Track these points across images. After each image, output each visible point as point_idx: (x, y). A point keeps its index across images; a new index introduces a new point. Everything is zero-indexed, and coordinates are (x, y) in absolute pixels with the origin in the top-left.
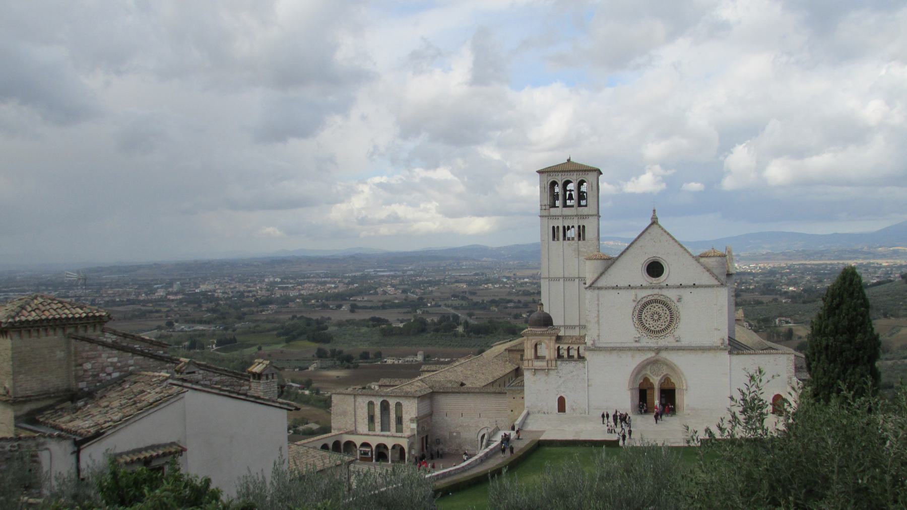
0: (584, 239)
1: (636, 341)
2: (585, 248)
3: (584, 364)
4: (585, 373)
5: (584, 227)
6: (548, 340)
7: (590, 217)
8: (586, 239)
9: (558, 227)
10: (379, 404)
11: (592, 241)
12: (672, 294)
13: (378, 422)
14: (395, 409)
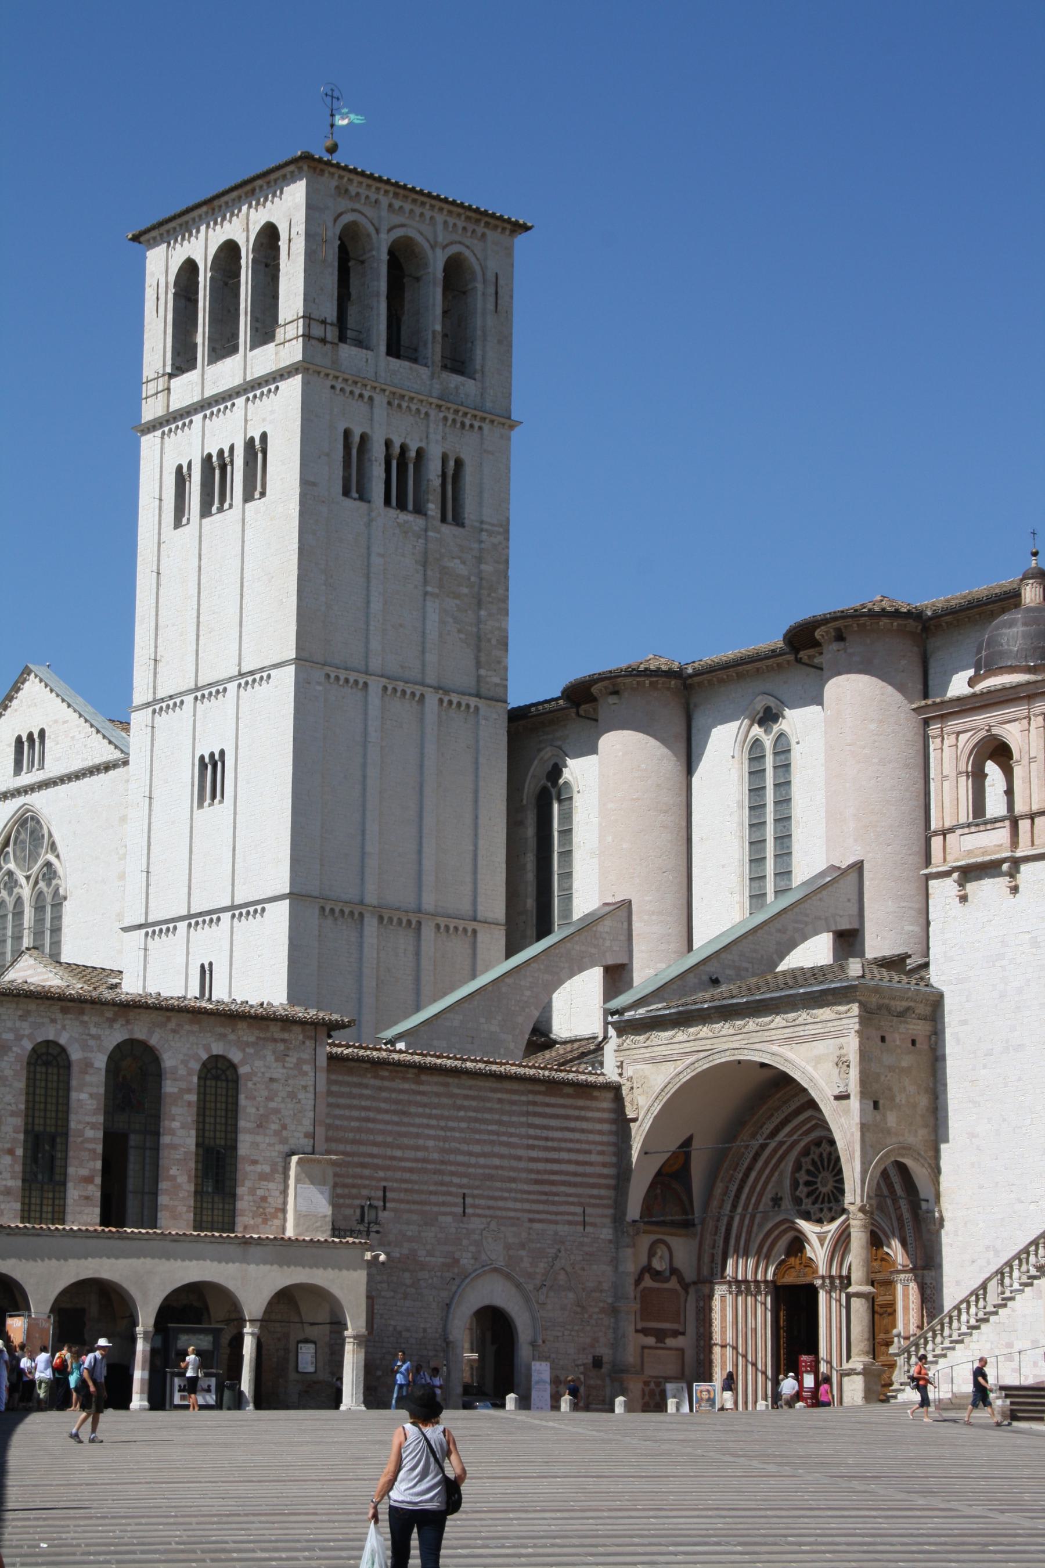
0: (458, 521)
2: (464, 563)
5: (459, 463)
7: (486, 427)
8: (467, 522)
9: (364, 438)
10: (100, 1061)
11: (491, 534)
13: (89, 1180)
14: (193, 1098)
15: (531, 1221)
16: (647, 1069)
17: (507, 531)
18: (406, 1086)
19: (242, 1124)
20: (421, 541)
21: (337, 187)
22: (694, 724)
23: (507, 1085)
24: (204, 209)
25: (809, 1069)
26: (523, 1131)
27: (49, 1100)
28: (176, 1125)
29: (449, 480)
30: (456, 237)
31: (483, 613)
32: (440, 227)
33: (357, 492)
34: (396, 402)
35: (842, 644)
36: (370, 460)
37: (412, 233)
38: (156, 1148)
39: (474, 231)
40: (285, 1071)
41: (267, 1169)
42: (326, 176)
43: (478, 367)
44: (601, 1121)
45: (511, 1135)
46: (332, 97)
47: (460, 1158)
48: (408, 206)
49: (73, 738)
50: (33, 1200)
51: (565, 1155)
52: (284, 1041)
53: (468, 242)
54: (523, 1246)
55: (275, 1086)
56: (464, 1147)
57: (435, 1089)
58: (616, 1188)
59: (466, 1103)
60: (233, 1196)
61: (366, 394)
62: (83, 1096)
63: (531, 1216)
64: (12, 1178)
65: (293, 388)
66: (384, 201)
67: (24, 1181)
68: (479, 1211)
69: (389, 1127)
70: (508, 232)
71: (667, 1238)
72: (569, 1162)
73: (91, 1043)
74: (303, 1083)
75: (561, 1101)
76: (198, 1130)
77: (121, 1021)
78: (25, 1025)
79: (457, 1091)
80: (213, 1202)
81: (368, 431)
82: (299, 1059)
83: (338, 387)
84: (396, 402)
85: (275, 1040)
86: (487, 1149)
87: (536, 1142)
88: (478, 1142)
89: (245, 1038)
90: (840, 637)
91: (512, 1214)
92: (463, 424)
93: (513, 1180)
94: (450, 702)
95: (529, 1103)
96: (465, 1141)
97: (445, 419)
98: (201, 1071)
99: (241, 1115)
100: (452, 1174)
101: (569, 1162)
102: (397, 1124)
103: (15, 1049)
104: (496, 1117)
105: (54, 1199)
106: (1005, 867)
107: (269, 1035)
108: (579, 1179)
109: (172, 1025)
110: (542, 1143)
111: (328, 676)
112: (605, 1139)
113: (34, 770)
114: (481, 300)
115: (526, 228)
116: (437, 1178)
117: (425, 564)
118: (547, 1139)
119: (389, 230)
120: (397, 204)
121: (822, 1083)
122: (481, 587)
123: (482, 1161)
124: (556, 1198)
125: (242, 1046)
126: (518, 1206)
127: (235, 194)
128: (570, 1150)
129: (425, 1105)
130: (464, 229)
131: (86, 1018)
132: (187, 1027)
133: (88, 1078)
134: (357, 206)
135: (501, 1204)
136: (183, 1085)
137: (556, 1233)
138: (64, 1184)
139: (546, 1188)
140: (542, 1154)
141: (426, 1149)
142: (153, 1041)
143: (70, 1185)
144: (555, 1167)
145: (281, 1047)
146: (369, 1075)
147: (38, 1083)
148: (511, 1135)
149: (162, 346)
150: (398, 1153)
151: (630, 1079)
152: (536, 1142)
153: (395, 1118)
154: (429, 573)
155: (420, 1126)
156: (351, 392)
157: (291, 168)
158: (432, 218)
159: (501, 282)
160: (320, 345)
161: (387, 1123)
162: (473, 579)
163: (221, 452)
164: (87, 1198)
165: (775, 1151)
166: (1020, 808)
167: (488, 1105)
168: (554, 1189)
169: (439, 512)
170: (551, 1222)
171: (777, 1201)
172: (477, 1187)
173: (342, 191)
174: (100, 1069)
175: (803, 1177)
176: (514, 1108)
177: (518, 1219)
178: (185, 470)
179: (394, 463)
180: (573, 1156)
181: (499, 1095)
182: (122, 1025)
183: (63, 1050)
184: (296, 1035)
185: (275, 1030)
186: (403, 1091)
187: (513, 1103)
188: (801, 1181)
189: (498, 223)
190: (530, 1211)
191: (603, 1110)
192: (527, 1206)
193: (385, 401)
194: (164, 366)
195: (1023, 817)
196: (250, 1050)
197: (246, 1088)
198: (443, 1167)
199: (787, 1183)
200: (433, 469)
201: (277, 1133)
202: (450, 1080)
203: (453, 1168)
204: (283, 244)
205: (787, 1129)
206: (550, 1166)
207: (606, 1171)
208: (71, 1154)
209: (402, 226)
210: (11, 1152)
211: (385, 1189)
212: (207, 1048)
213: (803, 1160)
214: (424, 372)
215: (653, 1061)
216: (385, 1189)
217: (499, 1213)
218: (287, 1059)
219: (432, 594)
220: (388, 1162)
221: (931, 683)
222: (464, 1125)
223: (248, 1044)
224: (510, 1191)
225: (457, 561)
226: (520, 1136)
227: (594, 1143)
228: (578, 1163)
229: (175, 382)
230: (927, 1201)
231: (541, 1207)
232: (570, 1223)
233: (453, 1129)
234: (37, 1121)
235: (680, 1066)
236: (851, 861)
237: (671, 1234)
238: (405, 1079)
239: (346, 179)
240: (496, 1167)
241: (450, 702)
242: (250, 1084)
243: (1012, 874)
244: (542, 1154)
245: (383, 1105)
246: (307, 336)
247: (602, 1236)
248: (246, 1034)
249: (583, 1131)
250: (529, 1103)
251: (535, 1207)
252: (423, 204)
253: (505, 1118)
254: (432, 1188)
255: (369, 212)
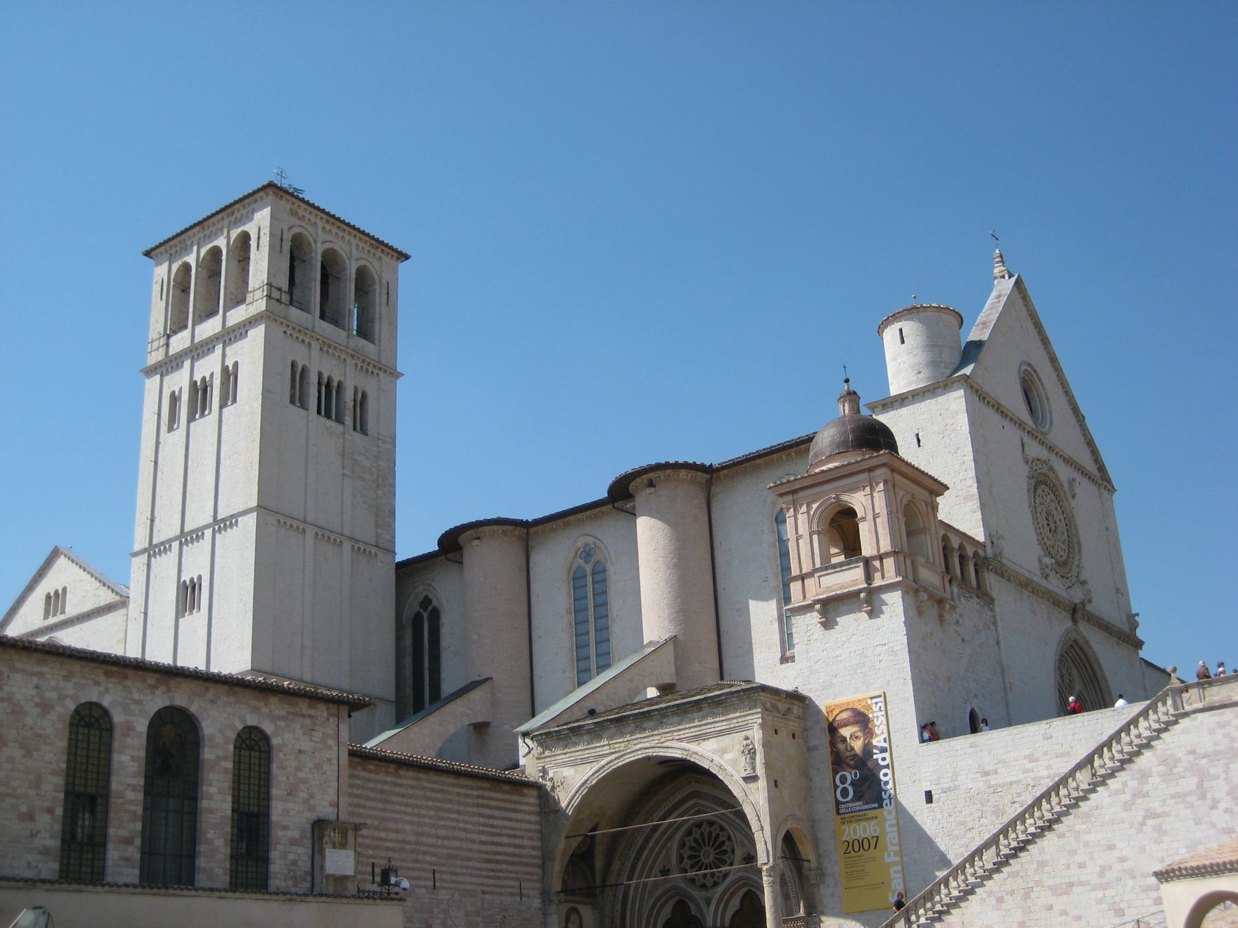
0: (364, 431)
1: (1047, 577)
3: (992, 610)
4: (998, 643)
5: (364, 395)
6: (926, 503)
7: (381, 374)
8: (369, 432)
9: (304, 370)
10: (142, 725)
12: (1064, 473)
15: (484, 892)
16: (568, 772)
17: (394, 443)
18: (388, 779)
19: (275, 791)
20: (341, 440)
21: (291, 209)
22: (531, 560)
23: (463, 781)
24: (197, 229)
25: (716, 758)
26: (475, 819)
27: (91, 761)
28: (213, 790)
29: (358, 405)
30: (363, 255)
31: (380, 492)
32: (354, 247)
33: (300, 402)
34: (325, 349)
35: (652, 490)
36: (308, 383)
37: (336, 247)
38: (194, 813)
39: (374, 254)
40: (312, 744)
41: (297, 834)
42: (283, 202)
43: (376, 337)
44: (530, 813)
45: (467, 822)
46: (281, 176)
47: (430, 840)
48: (335, 230)
49: (86, 591)
50: (72, 861)
51: (505, 840)
52: (311, 716)
53: (371, 260)
54: (478, 913)
55: (303, 757)
56: (433, 832)
57: (410, 782)
58: (542, 866)
59: (433, 795)
60: (266, 860)
61: (307, 340)
62: (125, 758)
63: (483, 888)
64: (51, 837)
65: (258, 334)
66: (320, 224)
67: (63, 841)
68: (445, 885)
69: (376, 813)
70: (395, 258)
71: (581, 908)
72: (509, 845)
73: (133, 707)
74: (328, 756)
75: (501, 796)
76: (233, 796)
77: (163, 688)
78: (69, 685)
79: (426, 784)
80: (247, 865)
81: (307, 364)
82: (324, 734)
83: (289, 333)
84: (325, 349)
85: (303, 716)
86: (450, 833)
87: (485, 829)
88: (444, 827)
89: (277, 712)
90: (651, 484)
91: (469, 887)
92: (367, 370)
93: (469, 859)
94: (359, 548)
95: (479, 797)
96: (433, 826)
97: (356, 365)
98: (236, 740)
99: (274, 783)
100: (425, 853)
101: (509, 845)
102: (383, 810)
103: (57, 708)
104: (456, 807)
105: (93, 860)
106: (862, 595)
107: (297, 710)
108: (516, 859)
109: (210, 695)
110: (489, 829)
111: (279, 521)
112: (533, 827)
113: (58, 614)
114: (379, 297)
115: (407, 257)
116: (413, 856)
117: (343, 456)
118: (492, 826)
119: (323, 243)
120: (328, 227)
121: (730, 769)
122: (378, 476)
123: (446, 843)
124: (501, 874)
125: (274, 719)
126: (474, 880)
127: (219, 216)
128: (509, 836)
129: (403, 795)
130: (369, 251)
131: (128, 683)
132: (224, 699)
133: (129, 741)
134: (303, 224)
135: (461, 878)
136: (221, 753)
137: (501, 903)
138: (103, 845)
139: (493, 866)
140: (490, 839)
141: (404, 831)
142: (193, 709)
143: (110, 846)
144: (499, 849)
145: (308, 722)
146: (360, 768)
147: (80, 744)
148: (467, 822)
149: (163, 318)
150: (383, 835)
151: (552, 779)
152: (485, 829)
153: (380, 805)
154: (346, 462)
155: (399, 812)
156: (297, 338)
157: (262, 193)
158: (349, 240)
159: (390, 288)
160: (278, 304)
161: (375, 809)
162: (373, 470)
163: (204, 379)
164: (127, 859)
165: (664, 833)
166: (867, 550)
167: (450, 797)
168: (499, 867)
169: (352, 423)
170: (498, 893)
171: (665, 872)
172: (443, 865)
173: (293, 213)
174: (142, 733)
175: (687, 853)
176: (468, 800)
177: (474, 891)
178: (177, 393)
179: (323, 388)
180: (511, 841)
181: (458, 790)
182: (163, 692)
183: (106, 713)
184: (321, 711)
185: (303, 705)
186: (385, 783)
187: (467, 796)
188: (685, 856)
189: (390, 251)
190: (482, 885)
191: (530, 804)
192: (480, 880)
193: (319, 347)
194: (165, 329)
195: (873, 558)
196: (282, 724)
197: (278, 758)
198: (418, 847)
199: (674, 858)
200: (349, 396)
201: (306, 802)
202: (421, 775)
203: (425, 848)
204: (253, 243)
205: (678, 812)
206: (495, 848)
207: (534, 853)
208: (112, 815)
209: (331, 242)
210: (50, 811)
211: (373, 864)
212: (242, 719)
213: (686, 839)
214: (343, 334)
215: (574, 764)
216: (373, 864)
217: (461, 886)
218: (314, 733)
219: (347, 476)
220: (375, 843)
221: (713, 517)
222: (432, 813)
223: (279, 718)
224: (468, 868)
225: (363, 457)
226: (474, 824)
227: (526, 830)
228: (515, 846)
229: (173, 340)
230: (809, 861)
231: (491, 882)
232: (511, 894)
233: (423, 816)
234: (77, 781)
235: (596, 766)
236: (667, 636)
237: (580, 903)
238: (387, 773)
239: (296, 205)
240: (457, 848)
241: (359, 548)
242: (281, 755)
243: (869, 601)
244: (490, 839)
245: (371, 794)
246: (269, 297)
247: (534, 905)
248: (277, 706)
249: (517, 820)
250: (479, 797)
251: (486, 881)
252: (344, 230)
253: (462, 808)
254: (410, 865)
255: (309, 228)
